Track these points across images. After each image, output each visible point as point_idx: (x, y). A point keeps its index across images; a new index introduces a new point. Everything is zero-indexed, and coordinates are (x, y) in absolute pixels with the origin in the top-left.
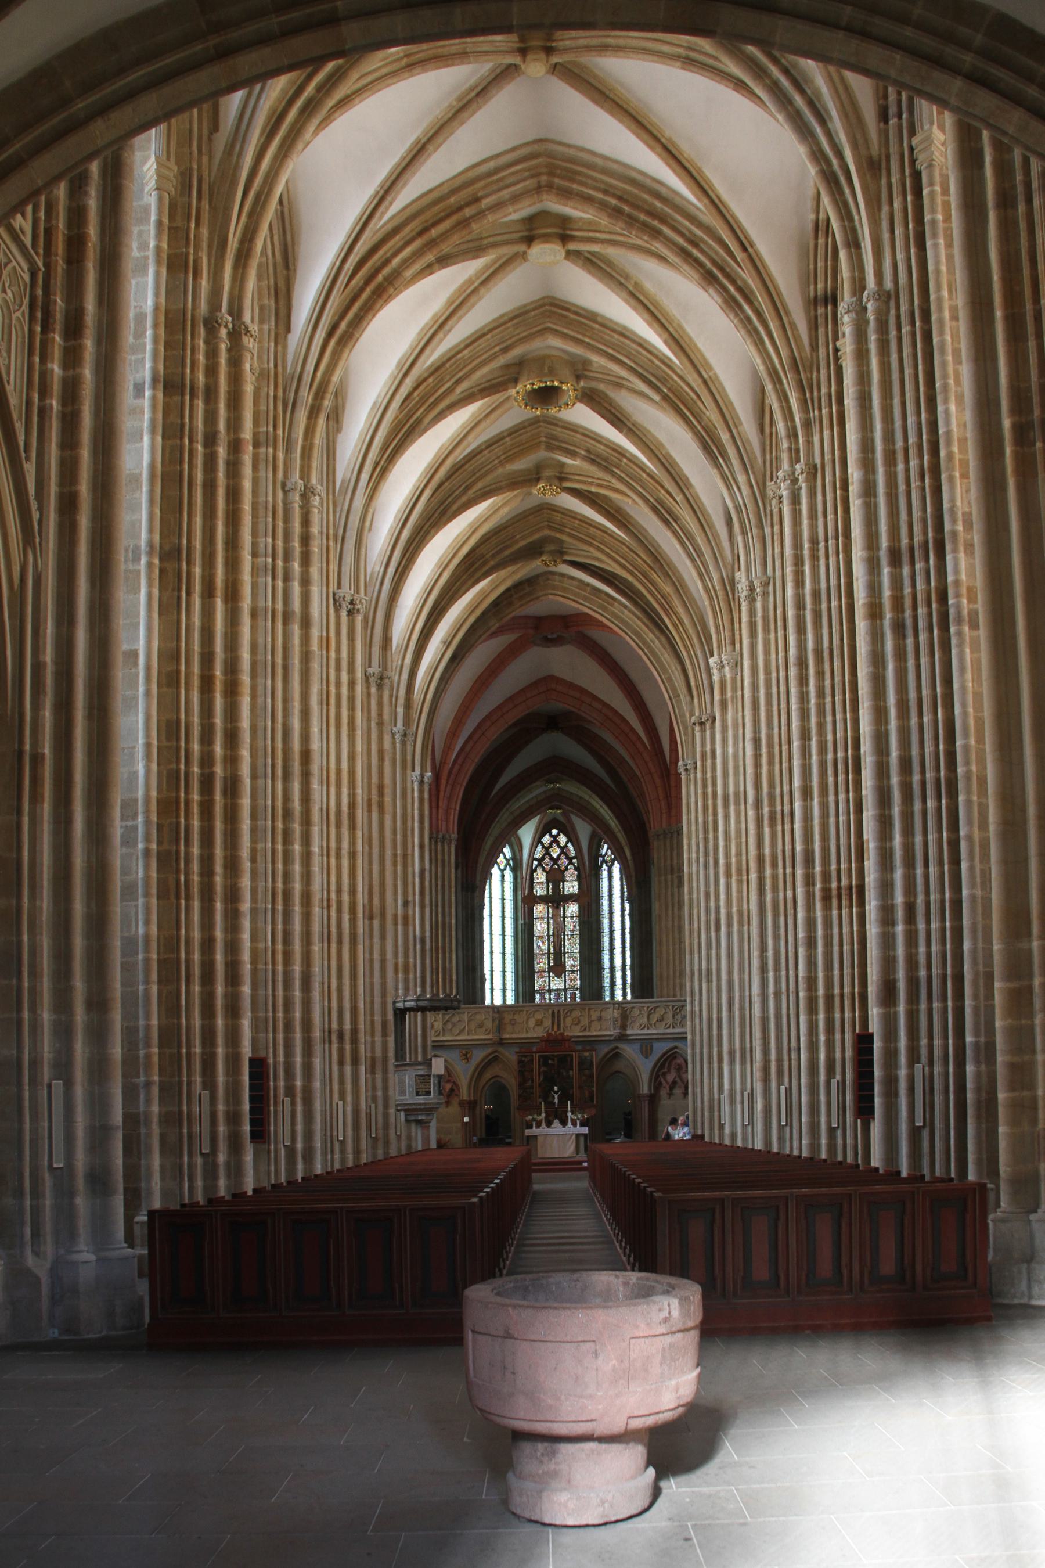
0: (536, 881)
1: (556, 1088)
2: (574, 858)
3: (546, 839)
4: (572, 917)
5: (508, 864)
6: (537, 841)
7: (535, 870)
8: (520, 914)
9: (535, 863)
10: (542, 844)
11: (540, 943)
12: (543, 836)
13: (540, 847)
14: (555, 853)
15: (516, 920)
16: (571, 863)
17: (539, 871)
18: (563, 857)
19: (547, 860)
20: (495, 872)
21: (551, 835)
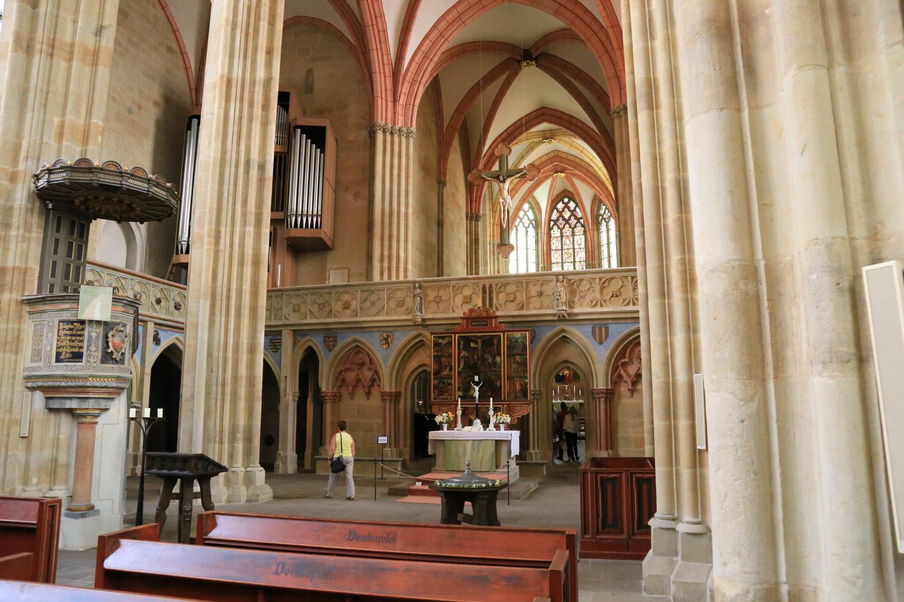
0: (553, 236)
2: (581, 218)
3: (560, 206)
5: (531, 223)
6: (553, 207)
7: (552, 228)
9: (552, 223)
10: (557, 209)
13: (555, 211)
14: (567, 214)
16: (578, 222)
17: (555, 228)
18: (573, 218)
19: (561, 220)
20: (521, 229)
21: (563, 203)
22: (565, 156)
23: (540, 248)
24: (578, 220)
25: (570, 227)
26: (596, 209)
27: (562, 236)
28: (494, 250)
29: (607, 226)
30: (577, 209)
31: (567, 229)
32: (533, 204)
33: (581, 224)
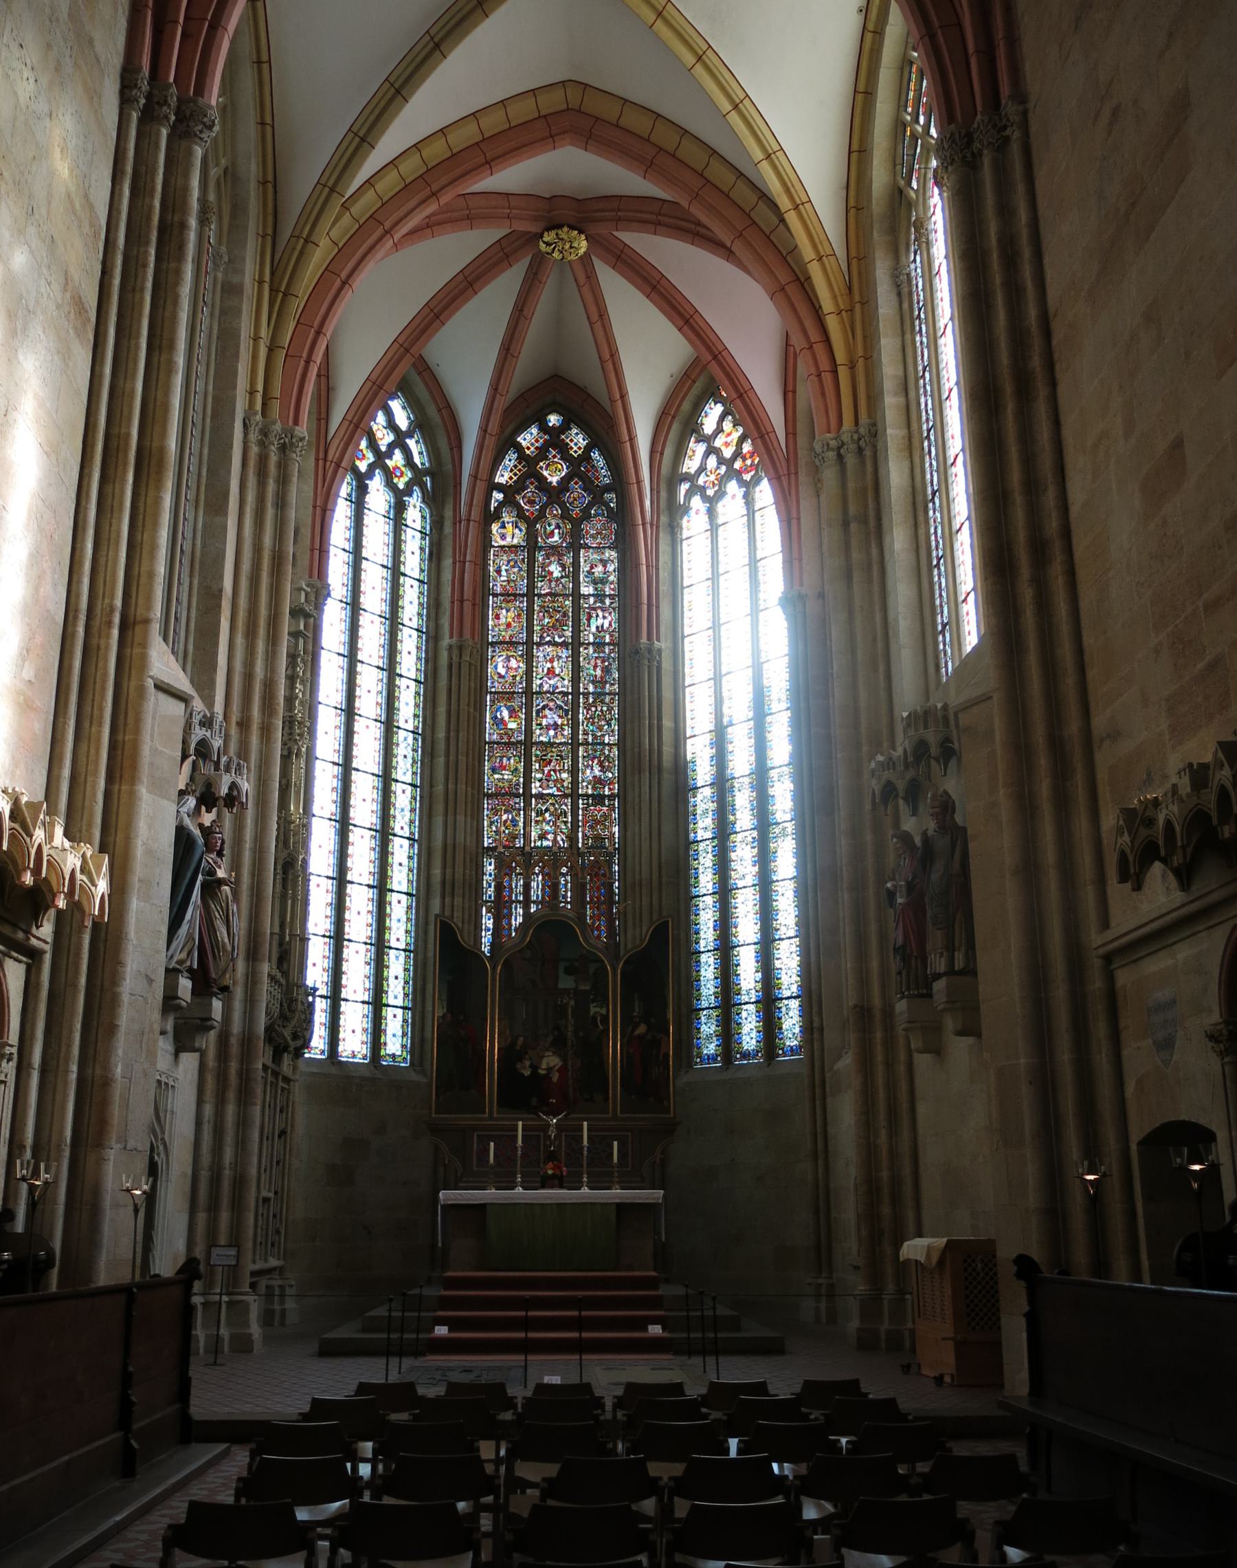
0: (497, 541)
1: (564, 870)
2: (608, 489)
3: (529, 438)
4: (599, 645)
5: (417, 480)
7: (497, 516)
8: (445, 622)
9: (498, 496)
10: (519, 448)
11: (506, 714)
12: (523, 427)
15: (431, 636)
18: (576, 487)
20: (378, 497)
21: (544, 428)
22: (610, 111)
23: (447, 576)
24: (596, 493)
25: (565, 516)
26: (669, 452)
27: (531, 544)
28: (263, 460)
29: (711, 513)
30: (595, 455)
31: (553, 522)
32: (432, 411)
33: (609, 509)
